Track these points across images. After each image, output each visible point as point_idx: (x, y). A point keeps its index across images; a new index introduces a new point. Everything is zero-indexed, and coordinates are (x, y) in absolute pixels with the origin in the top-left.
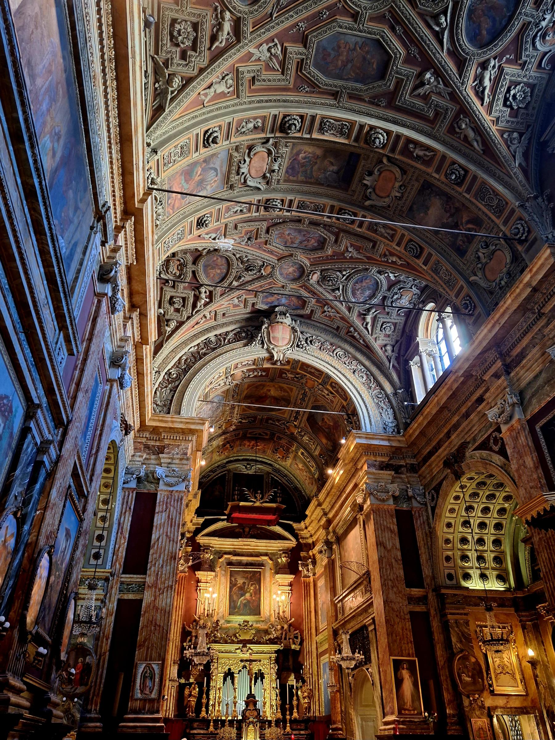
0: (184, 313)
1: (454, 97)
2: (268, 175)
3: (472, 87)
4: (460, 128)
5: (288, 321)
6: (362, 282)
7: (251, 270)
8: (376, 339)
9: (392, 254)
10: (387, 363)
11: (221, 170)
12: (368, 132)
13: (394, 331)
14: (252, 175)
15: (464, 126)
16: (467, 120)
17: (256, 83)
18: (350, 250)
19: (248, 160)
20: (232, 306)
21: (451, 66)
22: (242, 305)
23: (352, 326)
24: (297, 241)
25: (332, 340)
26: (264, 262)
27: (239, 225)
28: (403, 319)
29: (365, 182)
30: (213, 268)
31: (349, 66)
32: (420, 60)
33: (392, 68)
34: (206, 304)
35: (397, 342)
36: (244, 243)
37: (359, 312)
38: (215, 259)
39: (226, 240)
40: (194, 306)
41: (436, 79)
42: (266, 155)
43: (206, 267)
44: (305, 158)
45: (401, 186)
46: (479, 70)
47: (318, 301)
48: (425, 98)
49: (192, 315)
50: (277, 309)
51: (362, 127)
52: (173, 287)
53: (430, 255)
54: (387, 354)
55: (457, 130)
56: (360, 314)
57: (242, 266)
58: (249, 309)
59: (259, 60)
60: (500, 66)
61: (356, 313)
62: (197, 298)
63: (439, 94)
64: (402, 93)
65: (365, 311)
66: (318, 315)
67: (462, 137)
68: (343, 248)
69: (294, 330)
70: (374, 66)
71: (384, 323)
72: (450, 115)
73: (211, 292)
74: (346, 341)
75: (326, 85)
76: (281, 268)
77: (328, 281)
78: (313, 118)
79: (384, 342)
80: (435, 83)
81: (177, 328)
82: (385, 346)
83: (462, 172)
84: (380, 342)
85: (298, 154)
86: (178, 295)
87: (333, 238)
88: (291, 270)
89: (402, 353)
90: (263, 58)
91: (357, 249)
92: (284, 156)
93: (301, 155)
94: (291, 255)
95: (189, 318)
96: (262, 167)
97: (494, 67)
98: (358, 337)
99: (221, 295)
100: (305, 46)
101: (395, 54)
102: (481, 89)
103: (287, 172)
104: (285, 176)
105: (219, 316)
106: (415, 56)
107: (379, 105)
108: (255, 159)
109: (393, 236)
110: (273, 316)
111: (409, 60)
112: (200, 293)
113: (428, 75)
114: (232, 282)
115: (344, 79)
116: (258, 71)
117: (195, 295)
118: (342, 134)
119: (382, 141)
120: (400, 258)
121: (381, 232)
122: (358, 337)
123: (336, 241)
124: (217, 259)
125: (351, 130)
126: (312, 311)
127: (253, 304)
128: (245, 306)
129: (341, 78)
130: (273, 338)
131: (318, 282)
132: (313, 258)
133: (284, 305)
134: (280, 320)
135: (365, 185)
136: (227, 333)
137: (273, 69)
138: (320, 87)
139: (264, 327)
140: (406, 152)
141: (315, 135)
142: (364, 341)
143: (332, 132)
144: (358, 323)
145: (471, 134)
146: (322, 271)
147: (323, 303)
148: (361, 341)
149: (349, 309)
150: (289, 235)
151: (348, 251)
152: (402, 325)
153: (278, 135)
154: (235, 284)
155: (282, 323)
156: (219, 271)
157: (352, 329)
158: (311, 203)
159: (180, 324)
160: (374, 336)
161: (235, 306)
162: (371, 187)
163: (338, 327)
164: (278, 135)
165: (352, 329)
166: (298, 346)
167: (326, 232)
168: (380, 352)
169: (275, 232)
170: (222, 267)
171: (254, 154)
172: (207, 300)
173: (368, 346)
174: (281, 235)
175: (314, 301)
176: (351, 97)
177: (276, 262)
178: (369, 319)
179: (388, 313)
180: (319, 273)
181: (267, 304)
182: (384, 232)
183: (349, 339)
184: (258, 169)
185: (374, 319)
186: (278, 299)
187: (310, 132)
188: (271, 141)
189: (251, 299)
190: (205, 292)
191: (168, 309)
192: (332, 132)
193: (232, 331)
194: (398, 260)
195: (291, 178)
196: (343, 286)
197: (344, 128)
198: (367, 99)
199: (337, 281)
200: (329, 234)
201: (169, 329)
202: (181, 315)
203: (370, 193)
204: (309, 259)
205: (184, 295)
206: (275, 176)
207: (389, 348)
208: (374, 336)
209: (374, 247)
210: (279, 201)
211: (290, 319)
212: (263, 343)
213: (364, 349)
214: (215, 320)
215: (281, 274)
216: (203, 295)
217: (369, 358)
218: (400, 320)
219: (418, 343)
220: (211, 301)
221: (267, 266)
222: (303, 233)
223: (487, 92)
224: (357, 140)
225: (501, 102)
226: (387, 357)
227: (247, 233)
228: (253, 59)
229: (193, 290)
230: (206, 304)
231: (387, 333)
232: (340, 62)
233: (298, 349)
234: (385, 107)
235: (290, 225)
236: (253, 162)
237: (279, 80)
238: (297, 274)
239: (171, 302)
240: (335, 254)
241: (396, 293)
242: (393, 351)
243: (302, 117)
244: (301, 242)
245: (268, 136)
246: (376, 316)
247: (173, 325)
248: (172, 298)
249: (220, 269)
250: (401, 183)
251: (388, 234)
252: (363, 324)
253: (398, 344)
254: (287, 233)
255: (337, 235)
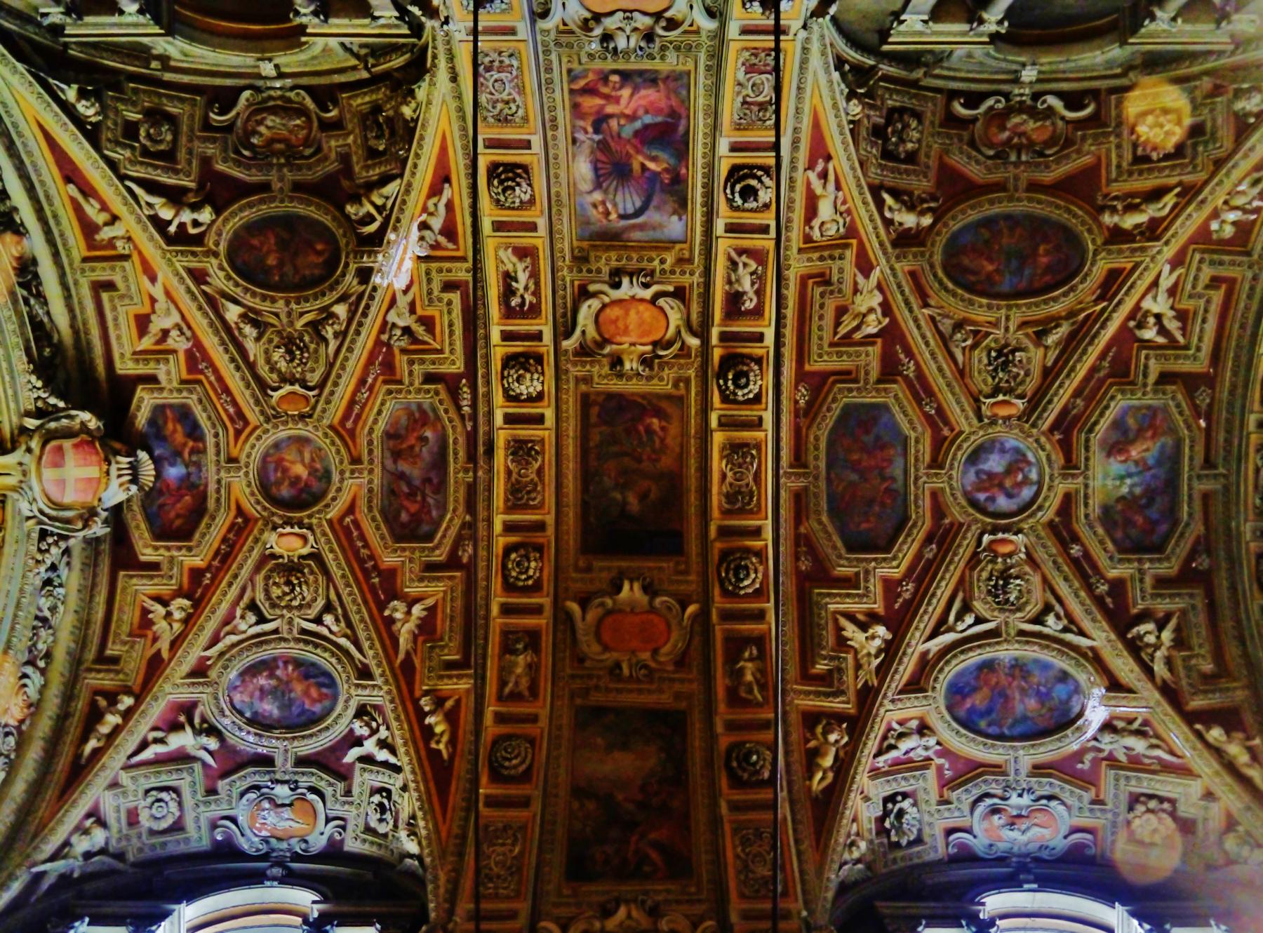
0: (128, 153)
1: (868, 697)
2: (607, 350)
3: (889, 724)
4: (826, 733)
5: (115, 493)
6: (306, 677)
7: (289, 352)
8: (114, 785)
9: (452, 718)
10: (49, 848)
11: (634, 227)
12: (749, 551)
13: (152, 833)
14: (608, 311)
15: (833, 737)
16: (846, 739)
17: (818, 290)
18: (417, 610)
19: (648, 294)
20: (146, 309)
21: (906, 668)
22: (147, 343)
23: (139, 699)
24: (403, 466)
25: (60, 655)
26: (321, 385)
27: (456, 297)
28: (205, 844)
29: (626, 586)
30: (283, 245)
31: (854, 477)
32: (897, 606)
33: (869, 561)
34: (160, 225)
35: (120, 856)
36: (392, 317)
37: (194, 705)
38: (319, 247)
39: (408, 264)
40: (152, 187)
41: (879, 651)
42: (656, 337)
43: (289, 222)
44: (649, 431)
45: (645, 666)
46: (914, 724)
47: (196, 574)
48: (842, 643)
49: (122, 178)
50: (143, 455)
51: (757, 532)
52: (207, 126)
53: (525, 803)
54: (74, 839)
55: (819, 729)
56: (188, 709)
57: (299, 324)
58: (126, 367)
59: (856, 291)
60: (929, 759)
61: (185, 695)
62: (175, 196)
63: (858, 666)
64: (836, 595)
65: (204, 720)
66: (140, 588)
67: (812, 744)
68: (413, 590)
69: (89, 515)
70: (864, 526)
71: (175, 790)
72: (837, 704)
73: (199, 240)
74: (68, 696)
75: (817, 439)
76: (302, 441)
77: (288, 583)
78: (758, 424)
79: (111, 818)
80: (873, 651)
81: (78, 121)
82: (102, 823)
83: (766, 775)
84: (110, 805)
85: (659, 413)
86: (183, 140)
87: (440, 556)
88: (300, 470)
89: (89, 887)
90: (858, 298)
91: (427, 627)
92: (655, 381)
93: (655, 421)
94: (356, 460)
95: (112, 165)
96: (626, 331)
97: (927, 748)
98: (104, 729)
99: (190, 272)
100: (879, 381)
101: (894, 558)
102: (893, 741)
103: (610, 396)
104: (598, 394)
105: (102, 273)
106: (899, 595)
107: (797, 559)
108: (647, 312)
109: (516, 697)
110: (117, 445)
111: (891, 587)
112: (195, 207)
113: (881, 630)
114: (236, 302)
115: (828, 473)
116: (840, 291)
117: (185, 190)
118: (730, 497)
119: (746, 583)
120: (452, 742)
121: (515, 664)
122: (104, 729)
123: (430, 567)
124: (319, 253)
125: (743, 512)
126: (155, 566)
127: (152, 379)
128: (139, 356)
129: (830, 466)
130: (60, 449)
131: (273, 556)
132: (356, 523)
133: (158, 476)
134: (114, 472)
135: (619, 589)
136: (41, 298)
137: (838, 323)
138: (809, 427)
139: (85, 416)
140: (736, 645)
141: (718, 438)
142: (97, 753)
143: (730, 474)
144: (155, 710)
145: (828, 761)
146: (316, 556)
147: (197, 589)
148: (92, 744)
149: (200, 671)
150: (424, 440)
151: (410, 606)
152: (183, 848)
153: (717, 353)
154: (233, 313)
155: (108, 473)
156: (271, 261)
157: (128, 701)
158: (540, 472)
159: (92, 134)
160: (124, 778)
161: (142, 323)
162: (615, 602)
163: (115, 660)
164: (717, 353)
165: (128, 701)
166: (43, 535)
167: (453, 532)
168: (75, 814)
169: (433, 399)
170: (288, 269)
171: (661, 309)
172: (172, 229)
173: (79, 771)
174: (420, 418)
175: (198, 562)
176: (799, 498)
177: (325, 422)
178: (184, 740)
179: (211, 791)
180: (306, 551)
181: (152, 422)
182: (519, 670)
183: (80, 705)
184: (621, 324)
185: (181, 758)
186: (178, 453)
187: (724, 424)
188: (694, 342)
189: (170, 372)
190: (196, 223)
191: (134, 104)
192: (730, 474)
193: (48, 313)
194: (445, 738)
195: (595, 410)
196: (276, 631)
197: (740, 501)
198: (802, 530)
199: (289, 607)
200: (448, 542)
201: (71, 93)
202: (118, 143)
203: (602, 604)
204: (351, 509)
205: (182, 155)
206: (599, 370)
207: (99, 837)
208: (124, 778)
209: (450, 665)
210: (539, 388)
211: (121, 497)
212: (39, 413)
213: (62, 764)
214: (85, 260)
215: (277, 445)
216: (187, 216)
217: (36, 789)
218: (198, 838)
219: (165, 915)
220: (170, 240)
221: (306, 398)
222: (433, 475)
223: (893, 754)
224: (724, 532)
225: (888, 790)
226: (67, 843)
227: (428, 322)
228: (860, 279)
229: (201, 186)
230: (160, 225)
231: (144, 818)
232: (856, 457)
233: (35, 535)
234: (798, 572)
235: (456, 437)
236: (642, 307)
237: (821, 338)
238: (285, 492)
239: (156, 116)
240: (390, 576)
241: (294, 786)
242: (88, 855)
243: (757, 399)
244: (402, 476)
245: (715, 332)
246: (195, 759)
247: (87, 110)
248: (172, 120)
249: (281, 264)
250: (653, 665)
251: (517, 683)
252: (154, 729)
253: (120, 866)
254: (429, 434)
255: (452, 563)
